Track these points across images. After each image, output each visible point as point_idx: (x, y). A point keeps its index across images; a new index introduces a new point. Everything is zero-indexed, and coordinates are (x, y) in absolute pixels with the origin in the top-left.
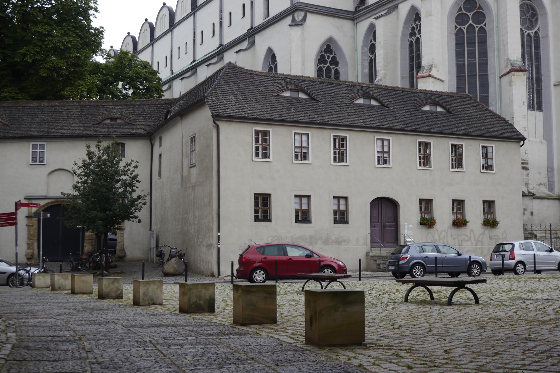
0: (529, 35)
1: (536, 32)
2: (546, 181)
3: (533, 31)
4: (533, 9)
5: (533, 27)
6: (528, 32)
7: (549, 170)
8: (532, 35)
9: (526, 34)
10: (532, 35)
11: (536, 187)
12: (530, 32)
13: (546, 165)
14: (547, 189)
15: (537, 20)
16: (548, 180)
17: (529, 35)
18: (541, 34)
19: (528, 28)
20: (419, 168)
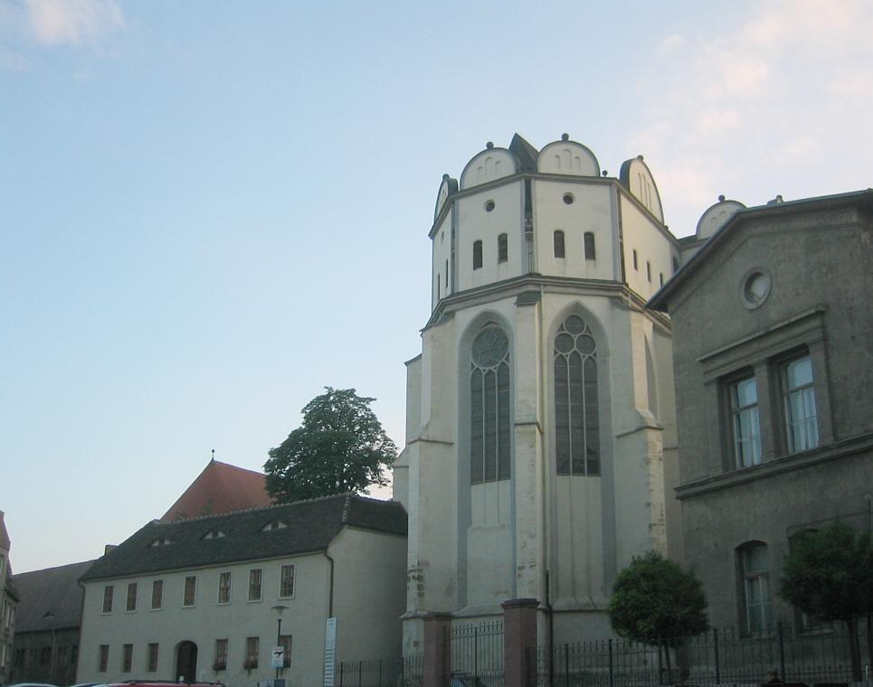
0: (490, 371)
3: (498, 365)
6: (487, 369)
8: (496, 371)
9: (484, 374)
10: (496, 371)
12: (492, 368)
17: (490, 371)
18: (510, 365)
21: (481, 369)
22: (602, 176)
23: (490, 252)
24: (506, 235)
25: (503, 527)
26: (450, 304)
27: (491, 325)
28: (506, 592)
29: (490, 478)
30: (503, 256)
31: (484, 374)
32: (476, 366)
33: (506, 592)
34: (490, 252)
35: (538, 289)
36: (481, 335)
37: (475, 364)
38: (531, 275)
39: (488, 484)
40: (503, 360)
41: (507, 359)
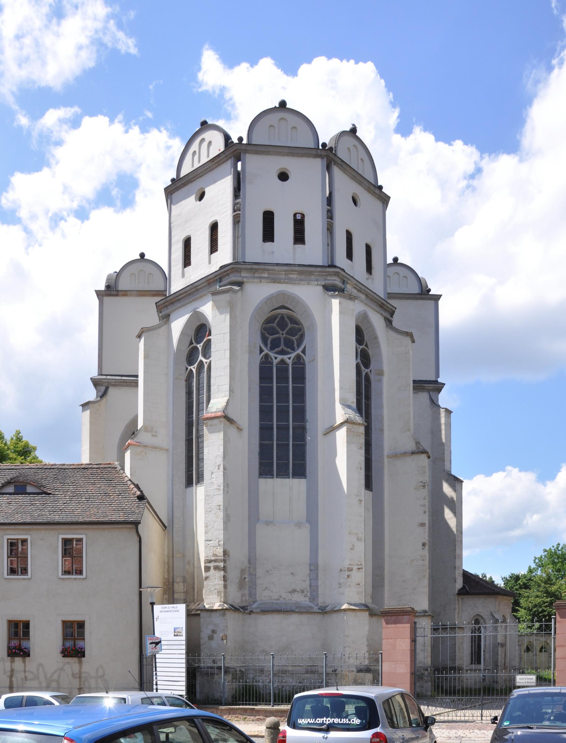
0: (283, 361)
1: (298, 357)
2: (306, 585)
3: (293, 355)
4: (294, 321)
5: (294, 349)
6: (280, 357)
7: (312, 568)
8: (290, 362)
9: (275, 362)
10: (290, 362)
11: (284, 595)
12: (285, 357)
13: (309, 562)
14: (307, 599)
15: (302, 338)
16: (311, 584)
17: (283, 361)
18: (306, 359)
19: (282, 352)
20: (29, 576)
21: (272, 355)
22: (320, 147)
23: (284, 228)
24: (303, 216)
25: (299, 525)
26: (228, 275)
27: (284, 311)
28: (303, 592)
29: (283, 473)
30: (299, 237)
31: (275, 362)
32: (266, 351)
33: (303, 592)
34: (284, 228)
35: (343, 286)
36: (270, 320)
37: (264, 348)
38: (329, 266)
39: (279, 480)
40: (299, 351)
41: (304, 352)
